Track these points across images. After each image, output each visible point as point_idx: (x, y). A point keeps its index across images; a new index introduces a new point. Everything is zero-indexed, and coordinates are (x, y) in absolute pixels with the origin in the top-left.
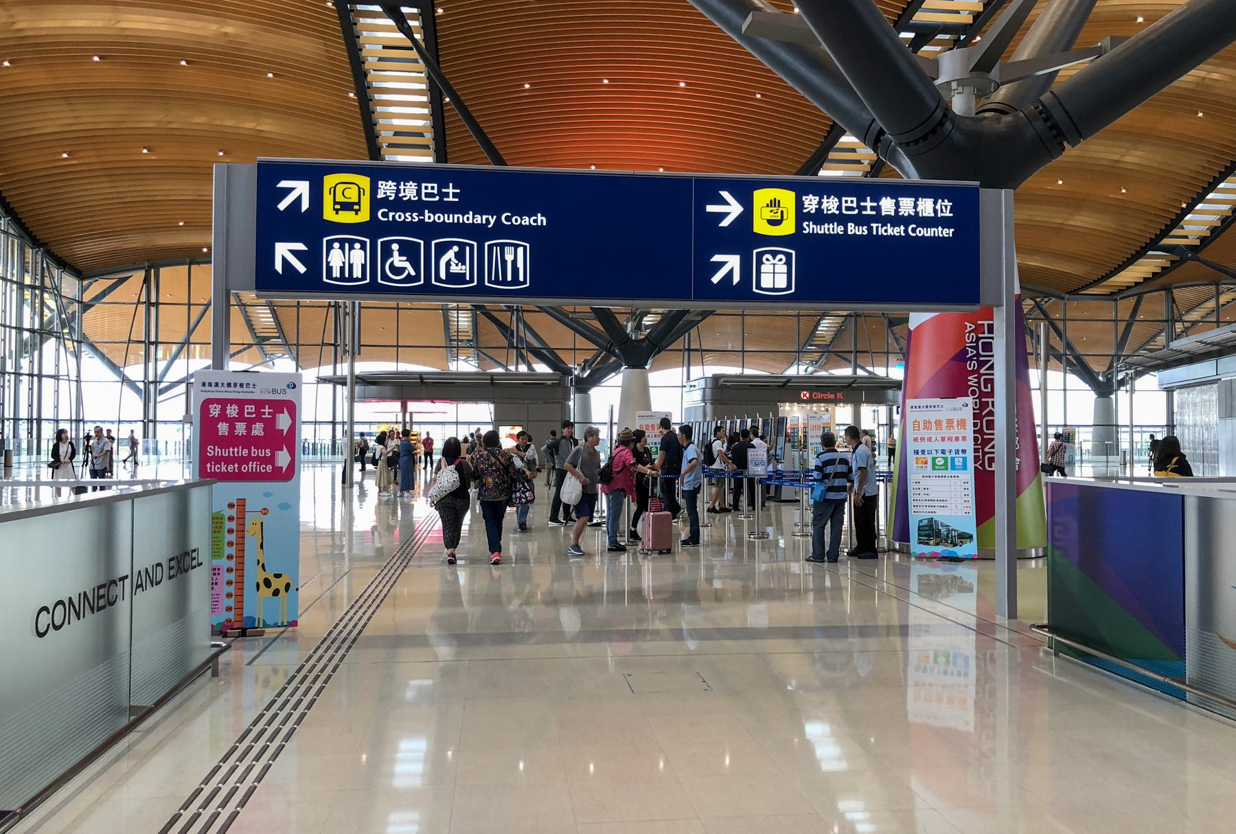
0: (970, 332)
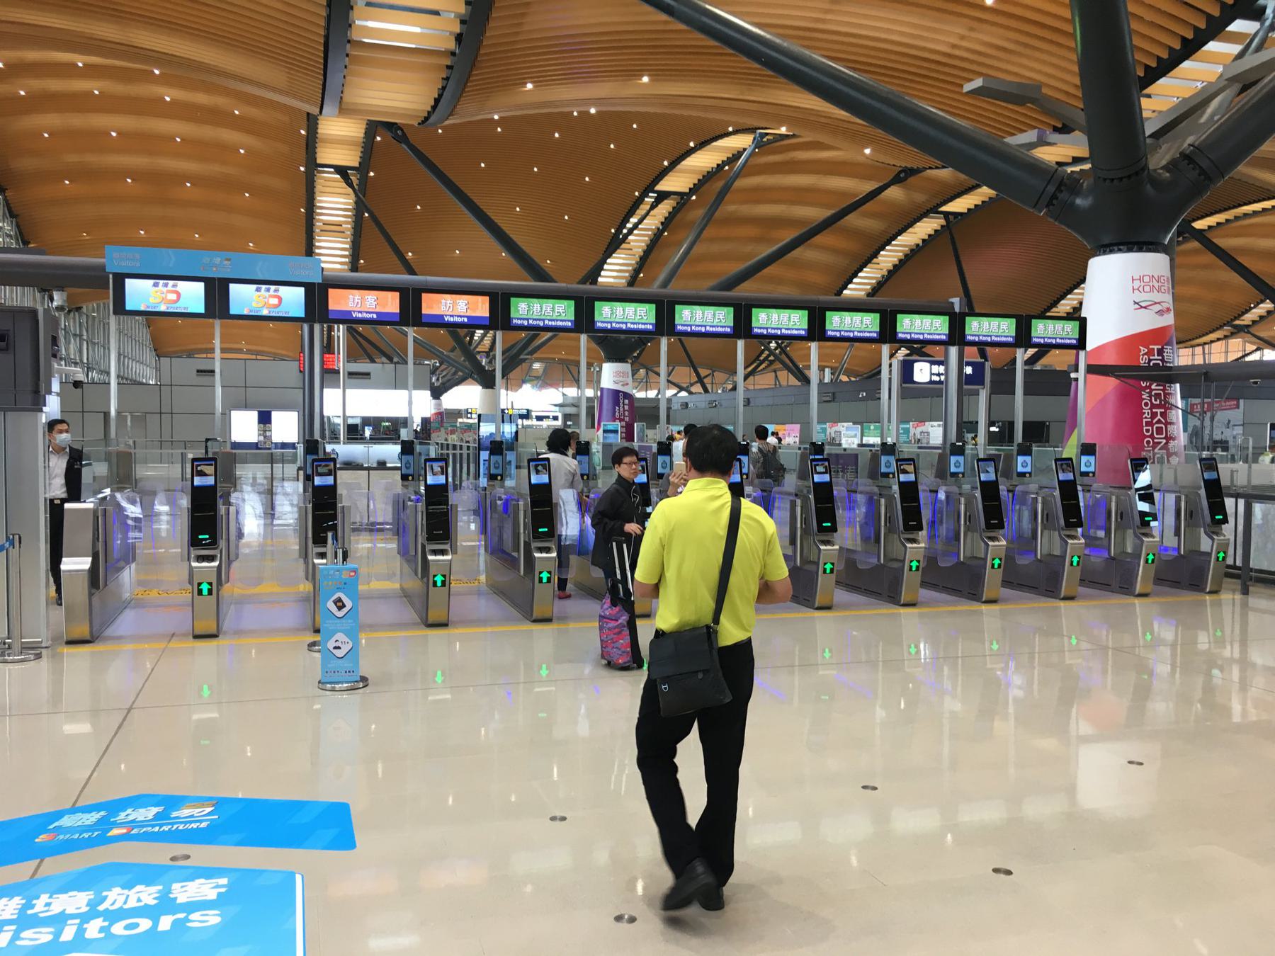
0: (1143, 355)
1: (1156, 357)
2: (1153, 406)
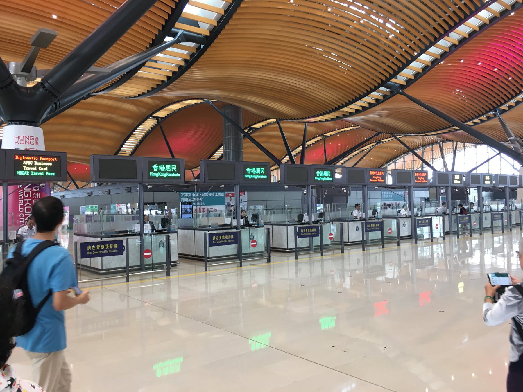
2: (24, 198)
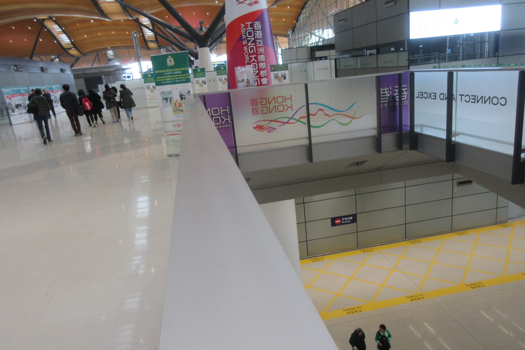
0: (243, 28)
1: (249, 28)
